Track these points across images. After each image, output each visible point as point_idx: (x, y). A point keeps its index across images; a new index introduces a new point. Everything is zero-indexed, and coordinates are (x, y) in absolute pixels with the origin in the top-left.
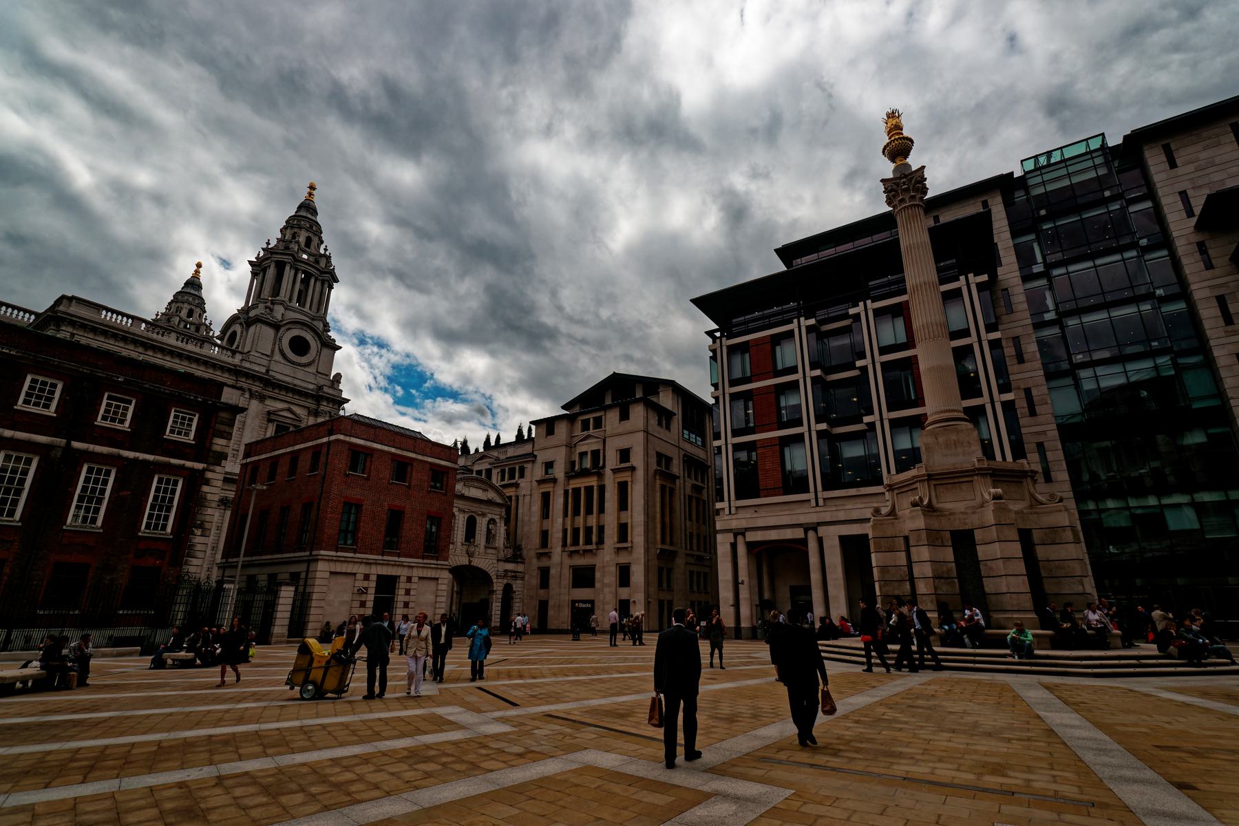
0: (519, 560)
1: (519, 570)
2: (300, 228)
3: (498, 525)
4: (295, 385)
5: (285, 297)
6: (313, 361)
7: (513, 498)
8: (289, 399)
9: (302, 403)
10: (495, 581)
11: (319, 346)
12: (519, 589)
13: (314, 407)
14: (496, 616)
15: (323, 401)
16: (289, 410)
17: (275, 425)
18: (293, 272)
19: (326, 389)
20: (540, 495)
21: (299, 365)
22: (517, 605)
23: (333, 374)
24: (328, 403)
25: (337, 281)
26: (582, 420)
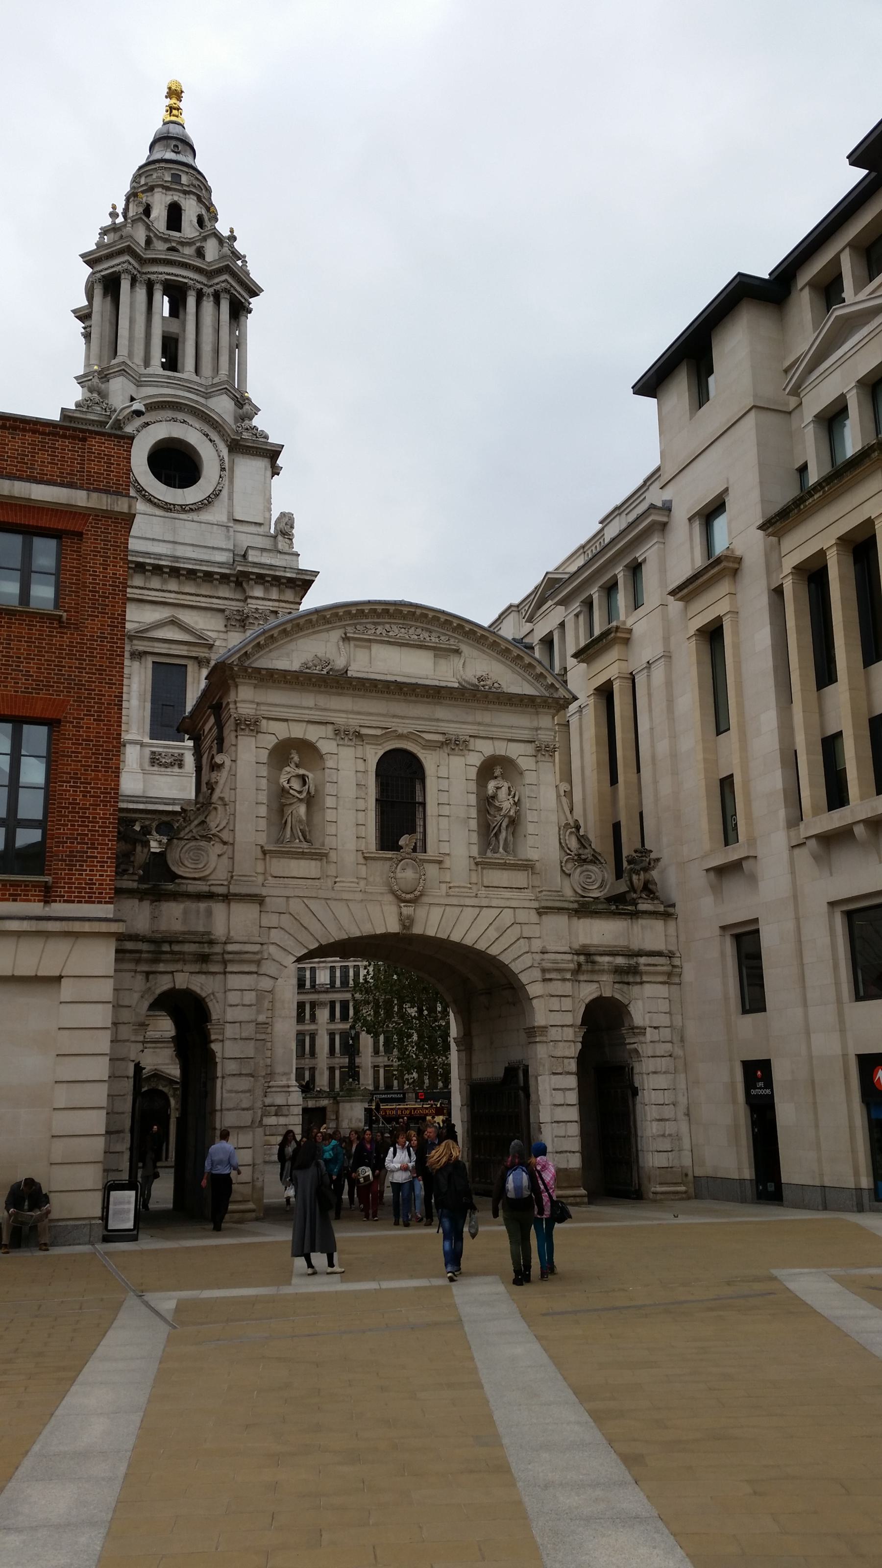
0: (643, 907)
1: (649, 946)
2: (151, 189)
3: (530, 778)
4: (176, 558)
5: (130, 355)
6: (216, 494)
7: (616, 686)
8: (171, 598)
9: (204, 602)
10: (534, 990)
11: (225, 452)
12: (664, 1020)
13: (235, 605)
14: (560, 1130)
15: (252, 588)
16: (173, 622)
17: (150, 665)
18: (141, 293)
19: (253, 556)
20: (693, 643)
21: (184, 509)
22: (661, 1081)
23: (275, 515)
24: (266, 590)
25: (254, 291)
26: (812, 284)
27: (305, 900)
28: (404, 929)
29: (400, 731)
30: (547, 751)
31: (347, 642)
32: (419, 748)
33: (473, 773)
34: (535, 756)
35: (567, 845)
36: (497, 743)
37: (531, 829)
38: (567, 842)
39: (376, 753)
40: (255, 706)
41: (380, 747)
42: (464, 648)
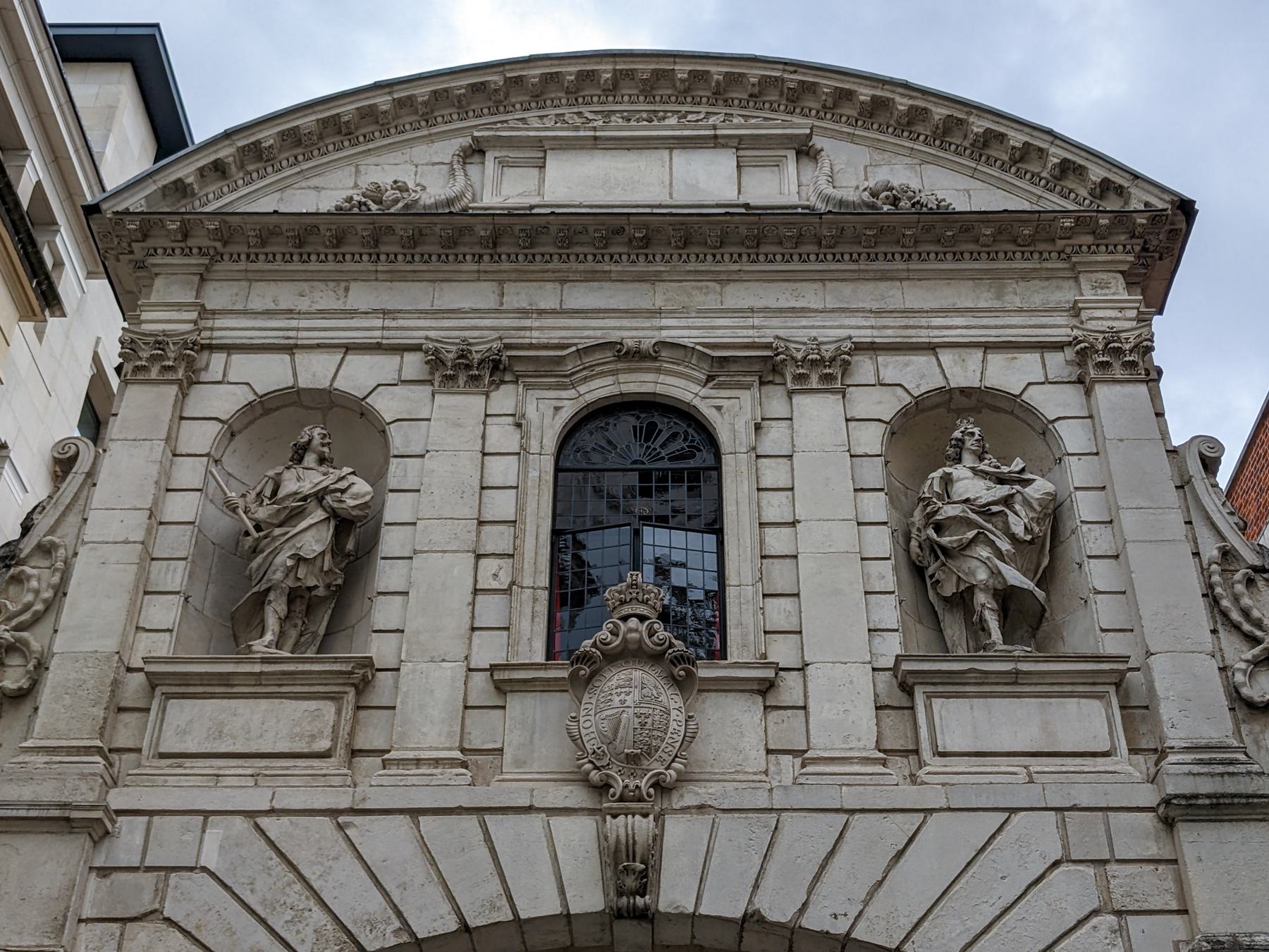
3: (1073, 436)
27: (264, 822)
28: (620, 894)
29: (630, 343)
30: (1118, 352)
31: (476, 158)
32: (695, 388)
33: (871, 439)
34: (1080, 381)
35: (1246, 613)
36: (946, 357)
37: (1099, 575)
38: (1246, 601)
39: (557, 409)
40: (194, 315)
41: (571, 393)
42: (818, 142)
